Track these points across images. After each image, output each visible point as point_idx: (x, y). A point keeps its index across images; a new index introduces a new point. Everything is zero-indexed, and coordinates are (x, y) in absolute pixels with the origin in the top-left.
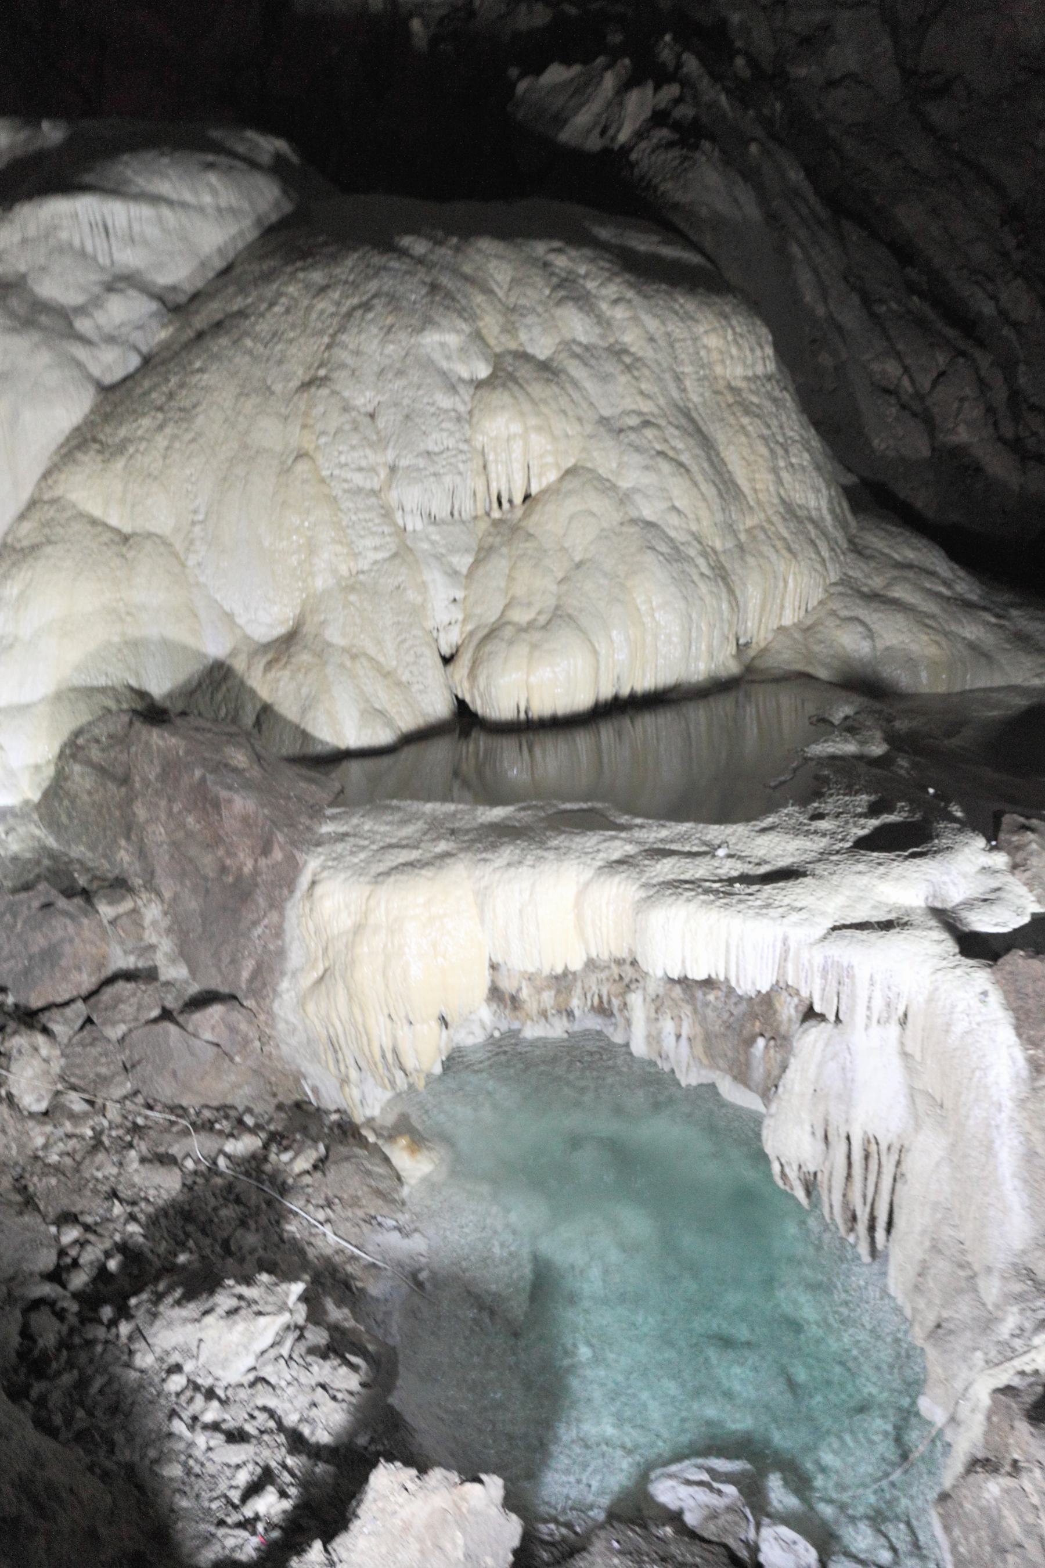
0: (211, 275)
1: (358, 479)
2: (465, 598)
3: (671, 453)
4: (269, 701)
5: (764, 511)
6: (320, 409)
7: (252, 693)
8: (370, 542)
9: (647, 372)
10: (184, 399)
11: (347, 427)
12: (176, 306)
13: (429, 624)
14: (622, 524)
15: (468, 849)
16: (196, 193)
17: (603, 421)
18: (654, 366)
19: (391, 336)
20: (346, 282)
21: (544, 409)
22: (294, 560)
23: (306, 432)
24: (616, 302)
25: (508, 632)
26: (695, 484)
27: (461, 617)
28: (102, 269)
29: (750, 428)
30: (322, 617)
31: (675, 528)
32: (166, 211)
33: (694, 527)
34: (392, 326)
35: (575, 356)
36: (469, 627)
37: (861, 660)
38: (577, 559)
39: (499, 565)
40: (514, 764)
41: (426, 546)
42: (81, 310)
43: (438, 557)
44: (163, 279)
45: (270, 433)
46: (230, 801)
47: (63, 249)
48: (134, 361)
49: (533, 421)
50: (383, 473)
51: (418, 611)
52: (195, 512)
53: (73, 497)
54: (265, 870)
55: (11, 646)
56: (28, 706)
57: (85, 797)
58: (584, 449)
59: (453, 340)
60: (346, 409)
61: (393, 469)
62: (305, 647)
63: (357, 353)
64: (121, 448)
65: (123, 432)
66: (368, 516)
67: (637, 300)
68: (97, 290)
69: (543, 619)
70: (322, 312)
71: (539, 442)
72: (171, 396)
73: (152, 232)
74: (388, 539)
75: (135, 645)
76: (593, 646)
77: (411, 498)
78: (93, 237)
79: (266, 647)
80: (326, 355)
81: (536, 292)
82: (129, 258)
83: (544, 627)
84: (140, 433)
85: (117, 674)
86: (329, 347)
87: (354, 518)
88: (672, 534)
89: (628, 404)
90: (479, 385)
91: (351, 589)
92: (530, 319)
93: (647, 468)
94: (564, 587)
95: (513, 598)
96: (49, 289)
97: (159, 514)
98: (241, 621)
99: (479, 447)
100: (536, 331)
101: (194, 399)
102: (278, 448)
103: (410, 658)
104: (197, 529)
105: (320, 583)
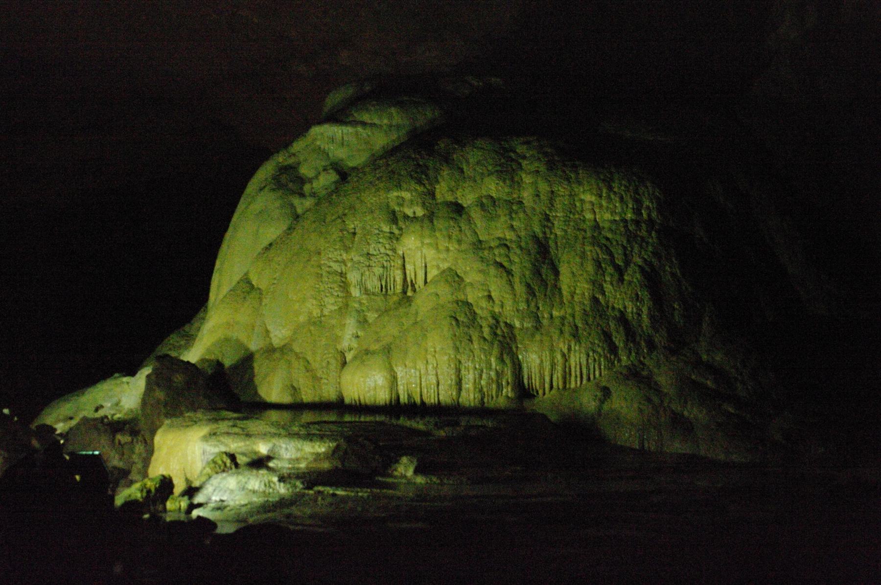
3: (506, 264)
5: (573, 309)
9: (522, 215)
13: (339, 347)
16: (380, 118)
18: (529, 212)
21: (438, 234)
26: (511, 284)
31: (482, 308)
32: (360, 129)
33: (497, 310)
41: (356, 305)
51: (337, 339)
71: (430, 253)
76: (391, 367)
88: (478, 311)
93: (480, 271)
98: (272, 335)
99: (401, 253)
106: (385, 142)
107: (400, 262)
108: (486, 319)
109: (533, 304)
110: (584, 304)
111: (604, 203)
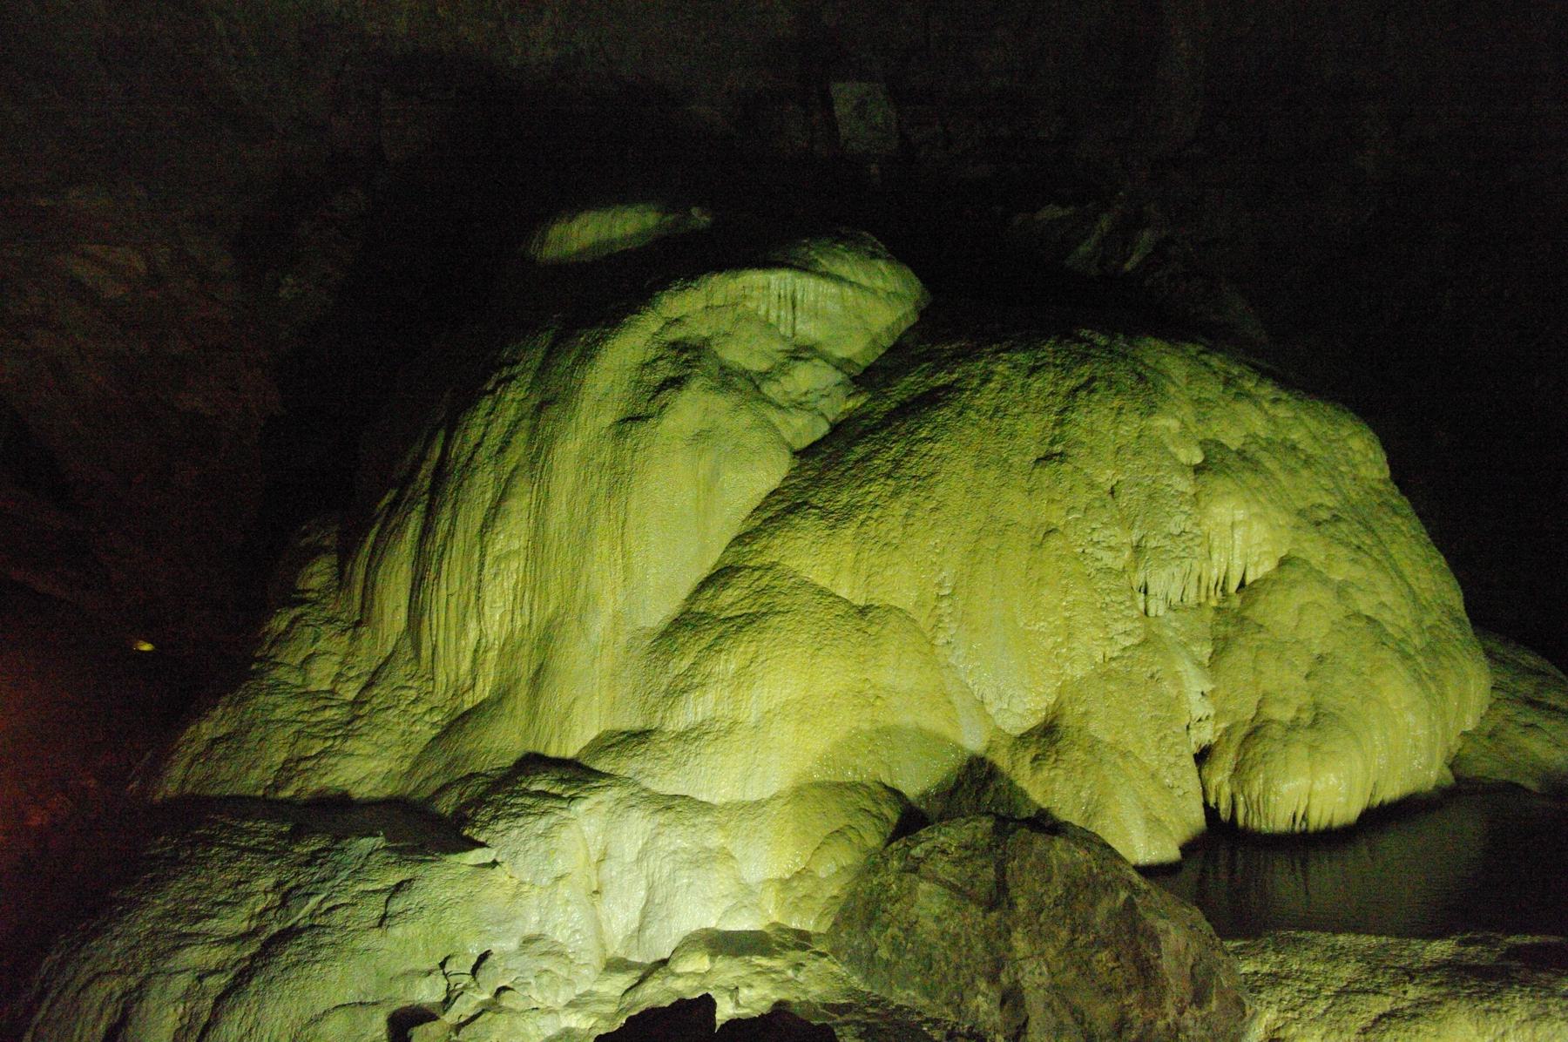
0: (881, 352)
1: (1108, 558)
2: (1213, 691)
4: (1045, 806)
6: (1067, 484)
7: (1023, 794)
8: (1120, 627)
10: (913, 466)
11: (1097, 504)
12: (865, 378)
14: (1348, 617)
15: (1455, 996)
17: (1301, 513)
19: (1123, 418)
20: (1056, 366)
22: (1049, 643)
23: (1054, 507)
24: (1275, 401)
25: (1276, 731)
27: (1212, 713)
28: (784, 338)
30: (1082, 710)
32: (848, 292)
34: (1121, 409)
35: (1265, 449)
36: (1223, 725)
37: (1558, 770)
38: (1317, 652)
39: (1240, 657)
40: (1283, 882)
42: (766, 375)
43: (1185, 645)
44: (840, 353)
45: (1017, 506)
46: (1167, 932)
47: (749, 318)
48: (823, 428)
49: (1255, 509)
50: (1127, 553)
51: (1173, 704)
52: (940, 585)
53: (792, 564)
54: (1190, 1023)
55: (729, 731)
56: (758, 804)
57: (931, 925)
58: (1295, 540)
59: (1174, 424)
60: (1092, 486)
61: (1138, 549)
62: (1073, 743)
63: (1092, 432)
64: (848, 513)
65: (844, 498)
66: (1120, 599)
67: (1293, 402)
68: (780, 357)
69: (1306, 717)
70: (1040, 391)
71: (1259, 531)
72: (897, 464)
73: (834, 308)
74: (1138, 624)
75: (886, 733)
77: (1166, 582)
78: (780, 309)
79: (1024, 739)
80: (1057, 432)
81: (1213, 390)
82: (809, 330)
83: (1314, 723)
84: (870, 498)
85: (868, 769)
86: (1059, 423)
87: (1108, 599)
89: (1317, 497)
90: (1198, 469)
91: (1106, 676)
92: (1217, 412)
94: (1314, 683)
95: (1265, 694)
96: (734, 354)
97: (899, 585)
98: (992, 710)
100: (1225, 423)
101: (930, 468)
102: (1026, 522)
103: (1172, 760)
104: (945, 603)
105: (1079, 671)
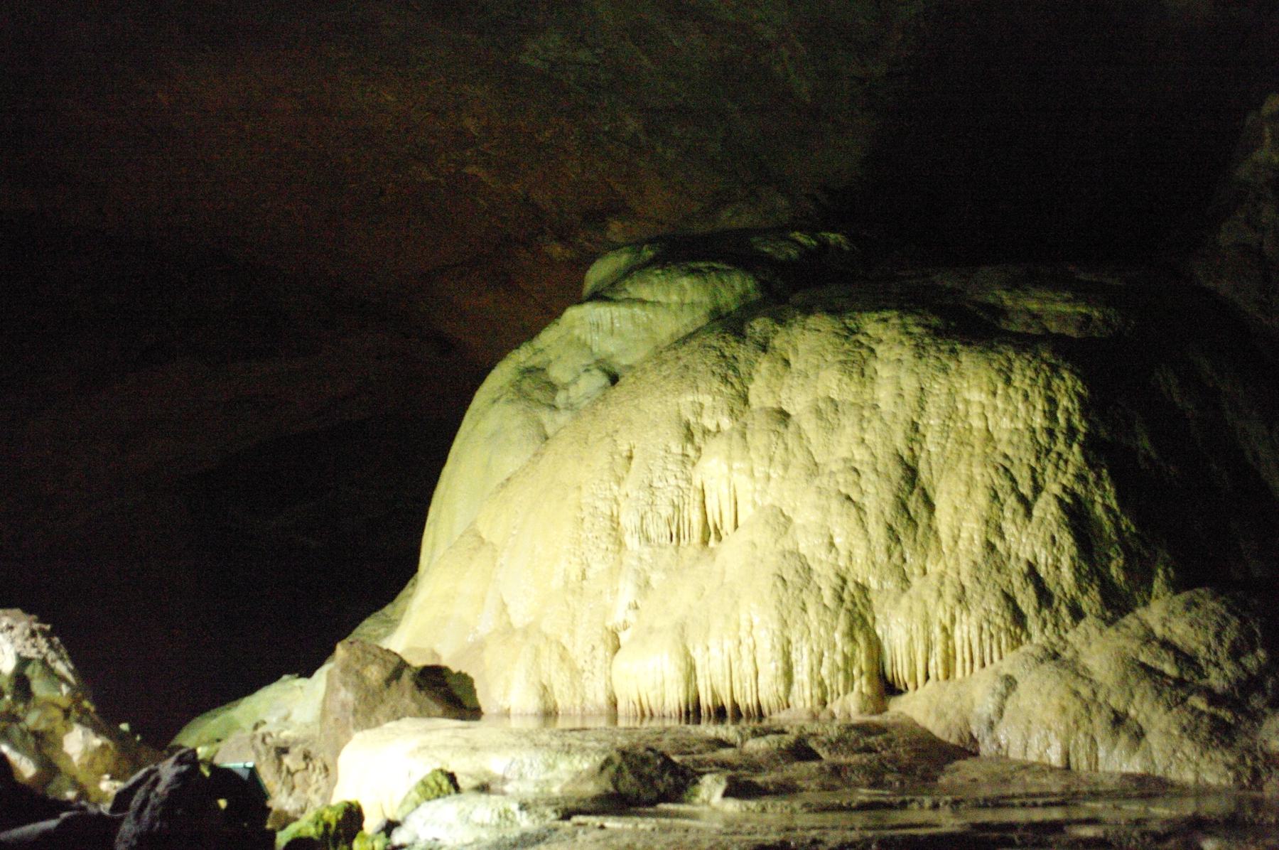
3: (855, 496)
5: (957, 559)
9: (877, 424)
16: (668, 294)
18: (887, 418)
26: (862, 523)
29: (978, 478)
31: (821, 562)
32: (637, 310)
33: (842, 563)
41: (635, 563)
88: (814, 566)
98: (510, 610)
106: (675, 329)
107: (698, 498)
108: (827, 577)
109: (896, 555)
110: (973, 553)
111: (999, 403)
